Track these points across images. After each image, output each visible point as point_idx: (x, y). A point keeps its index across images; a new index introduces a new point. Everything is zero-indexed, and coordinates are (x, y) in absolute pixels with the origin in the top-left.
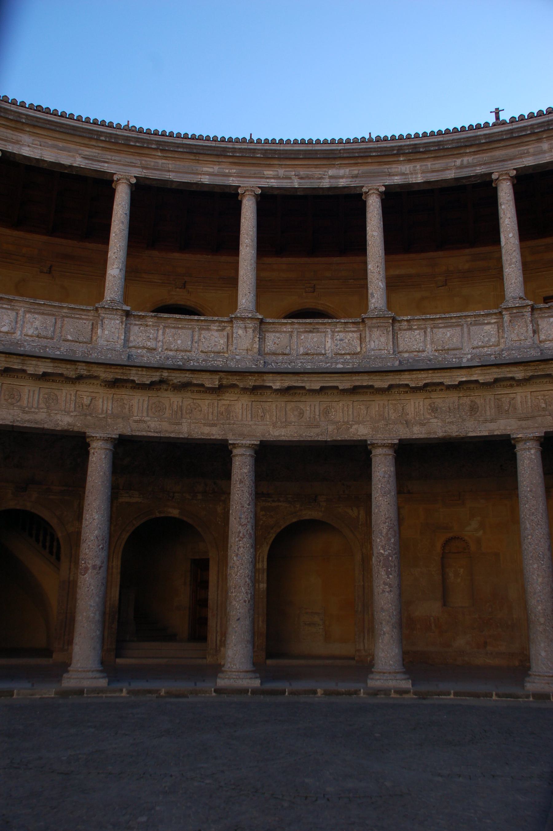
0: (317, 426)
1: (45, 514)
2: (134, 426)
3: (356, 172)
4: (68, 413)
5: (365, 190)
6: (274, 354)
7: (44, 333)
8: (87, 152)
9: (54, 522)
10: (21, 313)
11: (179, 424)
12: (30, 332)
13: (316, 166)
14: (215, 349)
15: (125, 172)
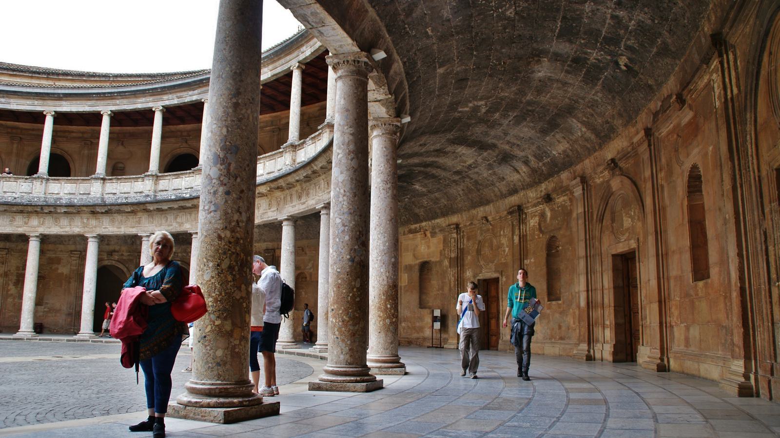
0: (172, 225)
1: (121, 266)
2: (104, 230)
3: (200, 91)
4: (78, 227)
5: (203, 101)
6: (163, 191)
7: (71, 192)
8: (90, 103)
9: (125, 270)
10: (63, 184)
11: (120, 228)
12: (66, 192)
13: (185, 91)
14: (140, 191)
15: (106, 109)
